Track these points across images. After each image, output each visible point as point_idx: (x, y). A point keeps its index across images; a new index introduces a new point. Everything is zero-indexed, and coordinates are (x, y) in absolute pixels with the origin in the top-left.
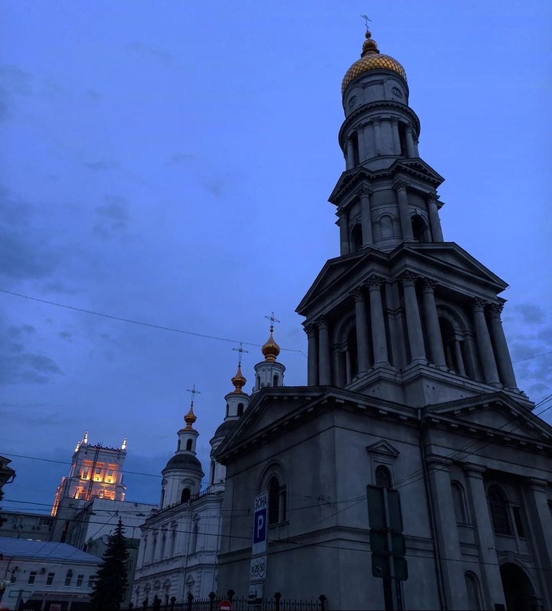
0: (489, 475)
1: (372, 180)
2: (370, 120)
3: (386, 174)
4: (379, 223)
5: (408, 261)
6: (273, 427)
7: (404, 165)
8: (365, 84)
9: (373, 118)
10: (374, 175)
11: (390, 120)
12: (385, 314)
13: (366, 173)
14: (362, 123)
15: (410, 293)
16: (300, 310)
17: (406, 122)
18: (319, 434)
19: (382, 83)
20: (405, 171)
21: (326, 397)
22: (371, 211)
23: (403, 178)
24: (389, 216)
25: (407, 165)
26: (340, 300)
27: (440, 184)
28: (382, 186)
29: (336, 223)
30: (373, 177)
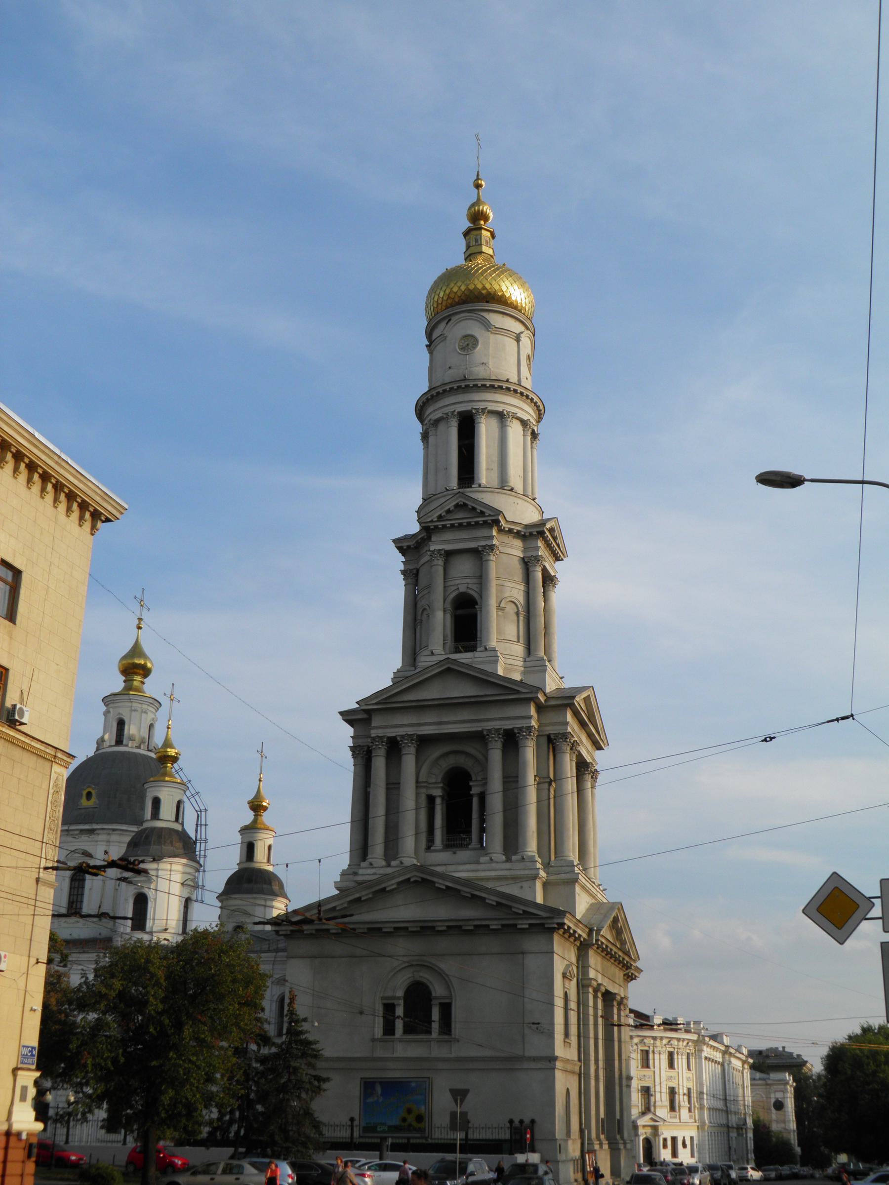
0: (608, 997)
1: (501, 530)
3: (521, 531)
4: (503, 609)
5: (569, 717)
6: (439, 924)
11: (524, 423)
14: (490, 408)
16: (367, 705)
18: (523, 953)
20: (545, 540)
21: (556, 921)
27: (562, 560)
28: (512, 547)
29: (394, 541)
30: (504, 528)
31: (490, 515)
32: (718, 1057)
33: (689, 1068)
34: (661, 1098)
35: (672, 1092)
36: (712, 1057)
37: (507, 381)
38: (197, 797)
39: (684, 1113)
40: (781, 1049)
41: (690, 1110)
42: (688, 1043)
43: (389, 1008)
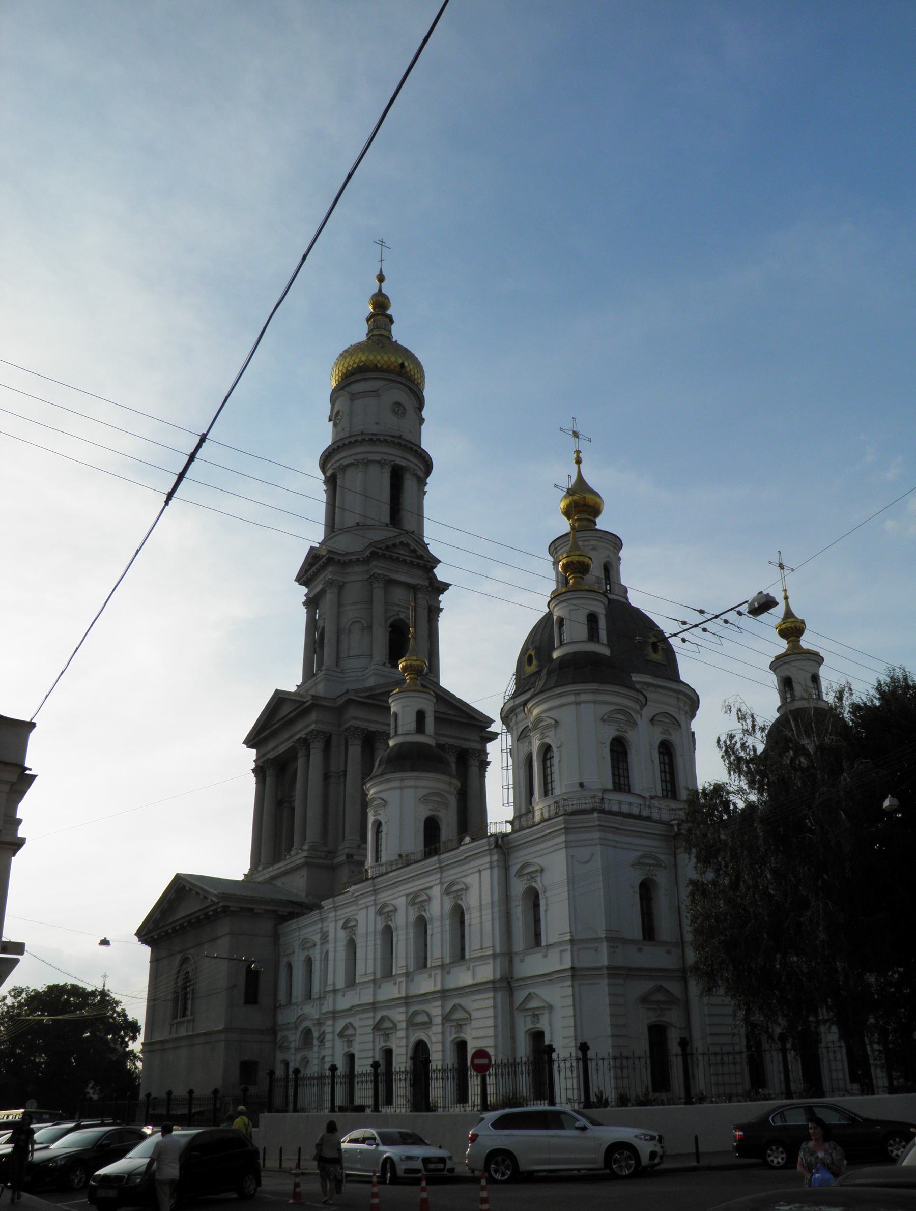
2: (352, 461)
7: (381, 548)
8: (353, 394)
9: (358, 460)
10: (347, 558)
11: (380, 463)
12: (326, 777)
13: (334, 556)
15: (355, 751)
17: (403, 463)
19: (375, 393)
22: (339, 613)
23: (378, 568)
24: (362, 623)
25: (387, 547)
26: (282, 749)
31: (325, 555)
37: (362, 433)
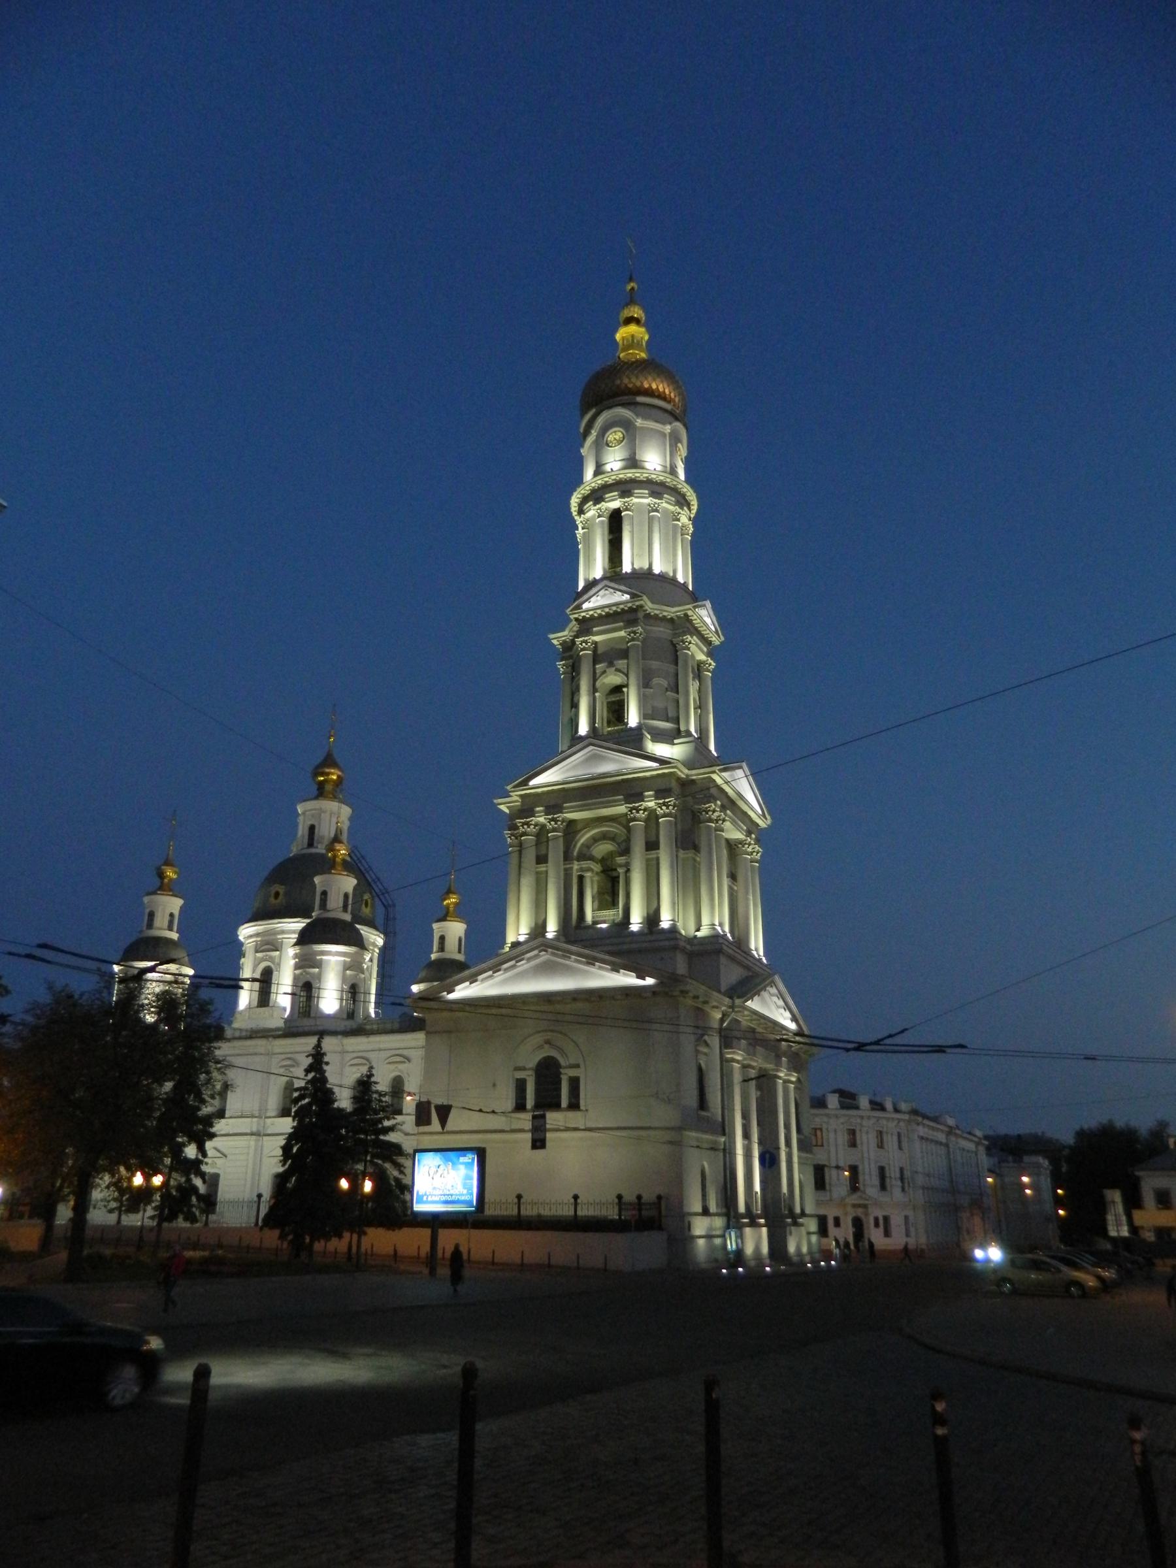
32: (941, 1137)
33: (900, 1148)
34: (869, 1179)
35: (882, 1171)
36: (930, 1137)
38: (386, 895)
39: (897, 1193)
40: (1040, 1134)
41: (903, 1190)
42: (899, 1122)
43: (521, 1086)
